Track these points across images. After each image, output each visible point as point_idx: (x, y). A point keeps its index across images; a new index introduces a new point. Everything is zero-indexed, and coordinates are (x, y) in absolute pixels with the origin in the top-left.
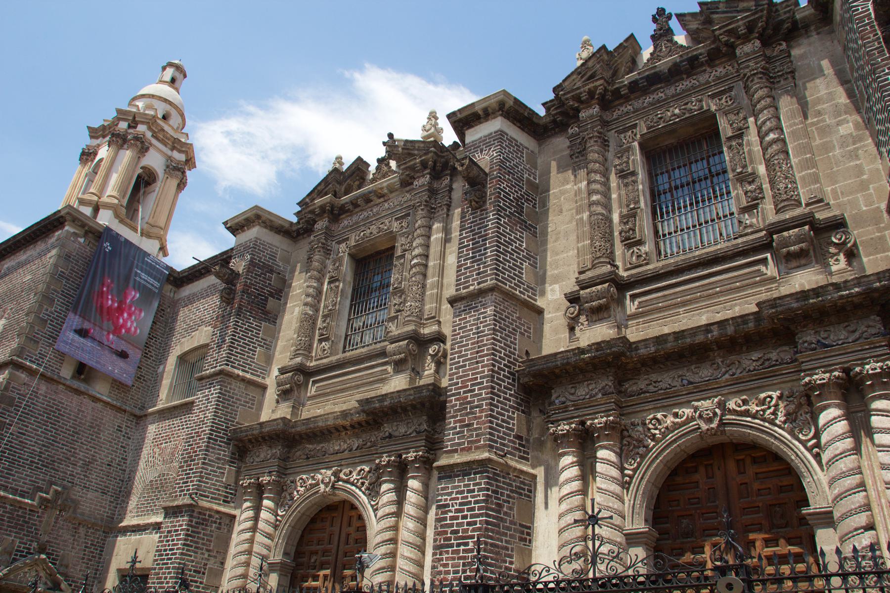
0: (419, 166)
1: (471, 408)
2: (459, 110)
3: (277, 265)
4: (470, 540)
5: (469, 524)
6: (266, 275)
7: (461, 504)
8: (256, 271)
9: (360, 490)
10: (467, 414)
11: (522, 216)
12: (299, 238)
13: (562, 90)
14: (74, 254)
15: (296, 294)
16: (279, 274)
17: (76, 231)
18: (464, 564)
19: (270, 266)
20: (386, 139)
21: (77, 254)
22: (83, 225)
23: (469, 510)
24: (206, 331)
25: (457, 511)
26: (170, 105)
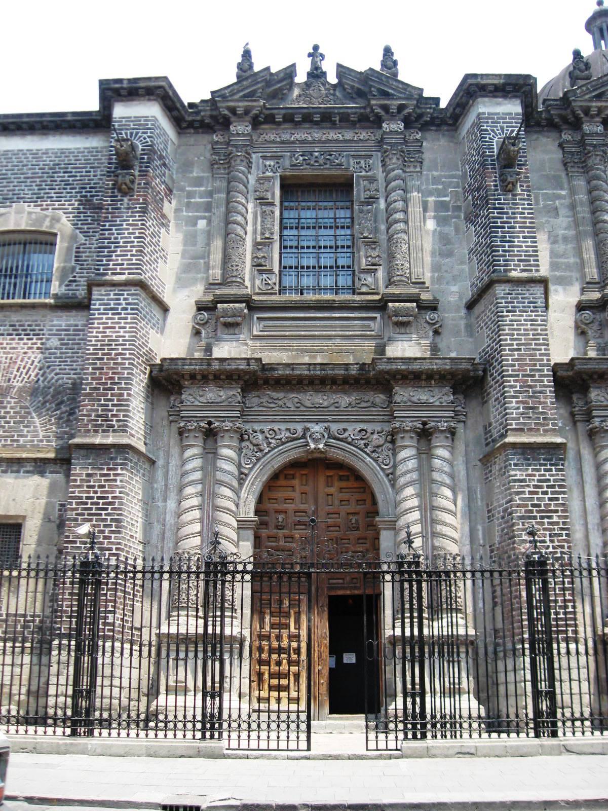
0: (393, 109)
1: (534, 392)
2: (482, 75)
4: (554, 514)
5: (550, 499)
7: (539, 481)
9: (365, 452)
10: (530, 397)
12: (188, 131)
13: (574, 96)
15: (197, 203)
18: (550, 536)
20: (312, 51)
23: (548, 487)
24: (30, 213)
25: (535, 486)
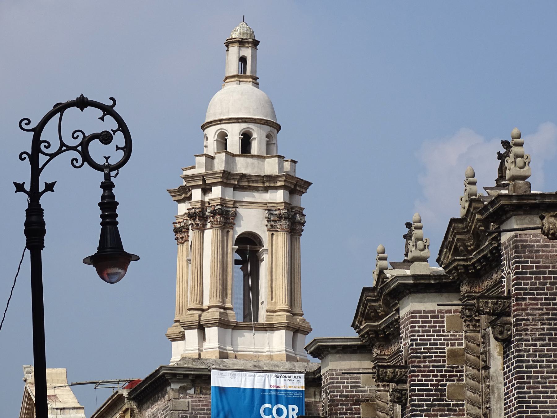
3: (362, 391)
6: (352, 409)
8: (340, 409)
11: (443, 400)
14: (190, 411)
16: (367, 400)
17: (183, 385)
19: (354, 396)
21: (192, 409)
22: (186, 376)
26: (246, 122)
